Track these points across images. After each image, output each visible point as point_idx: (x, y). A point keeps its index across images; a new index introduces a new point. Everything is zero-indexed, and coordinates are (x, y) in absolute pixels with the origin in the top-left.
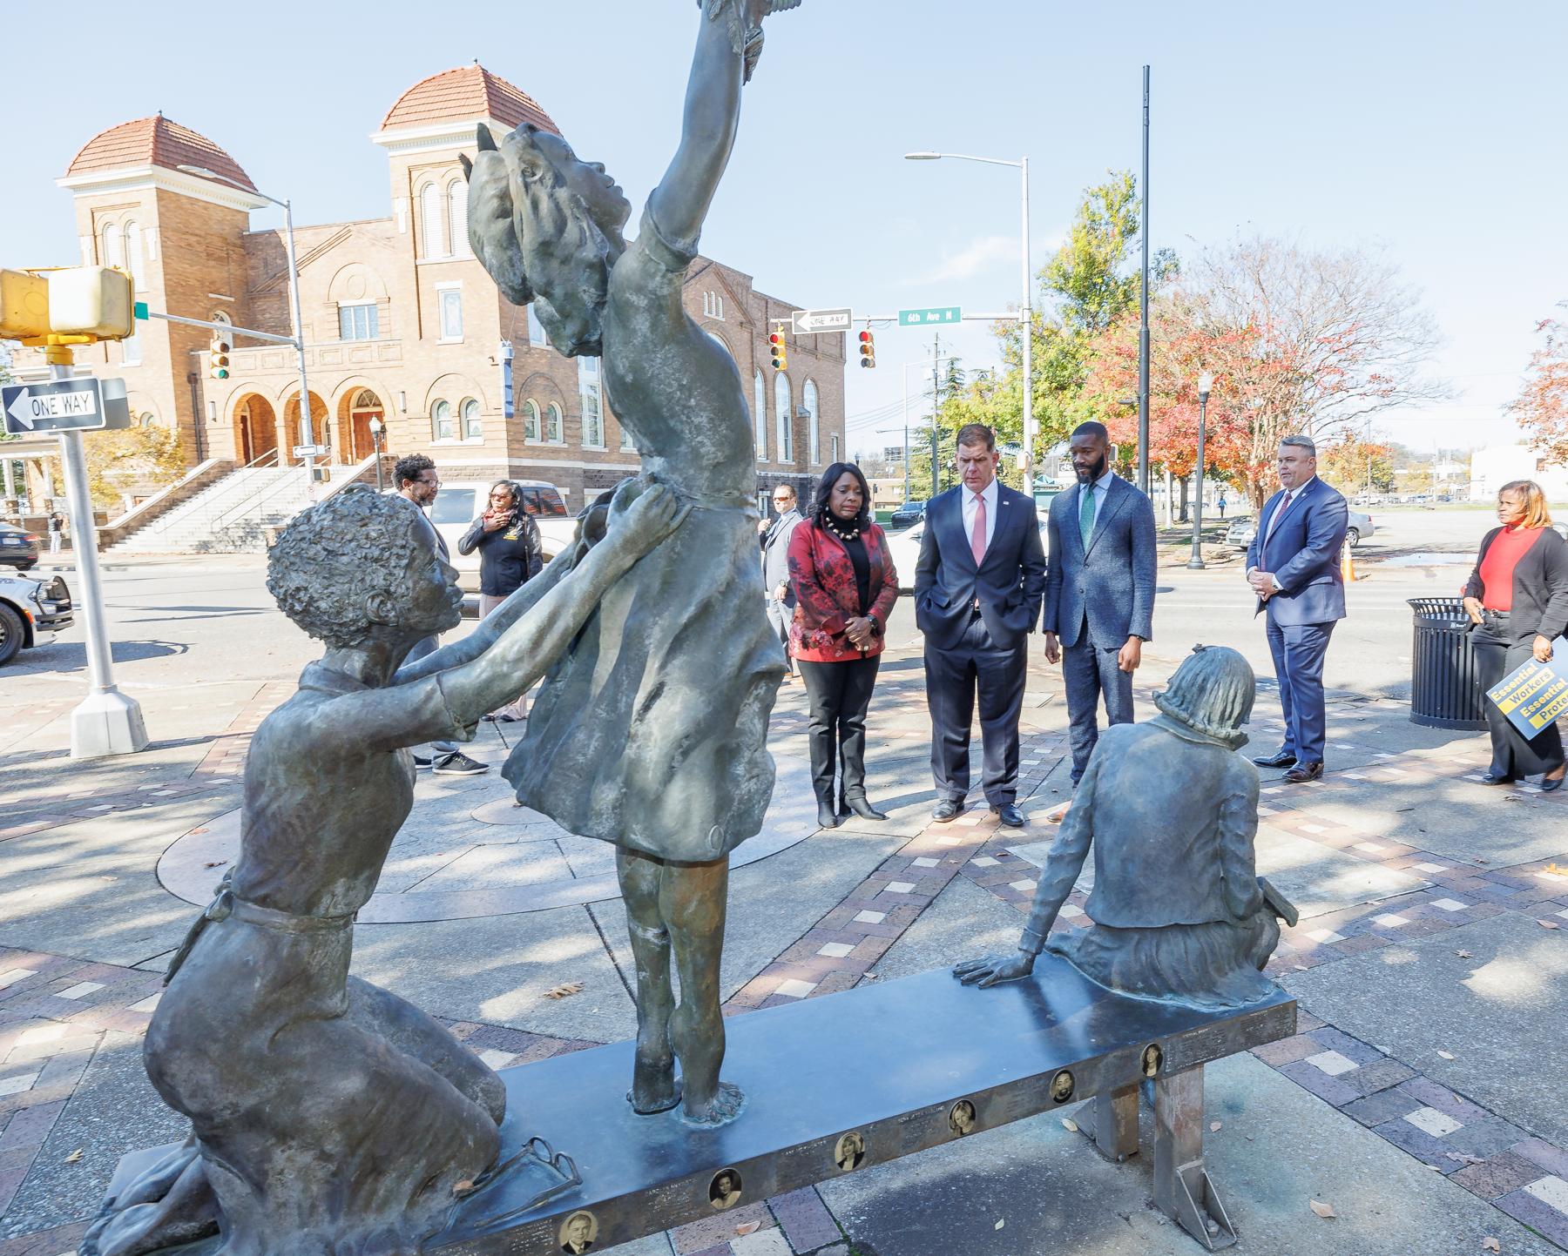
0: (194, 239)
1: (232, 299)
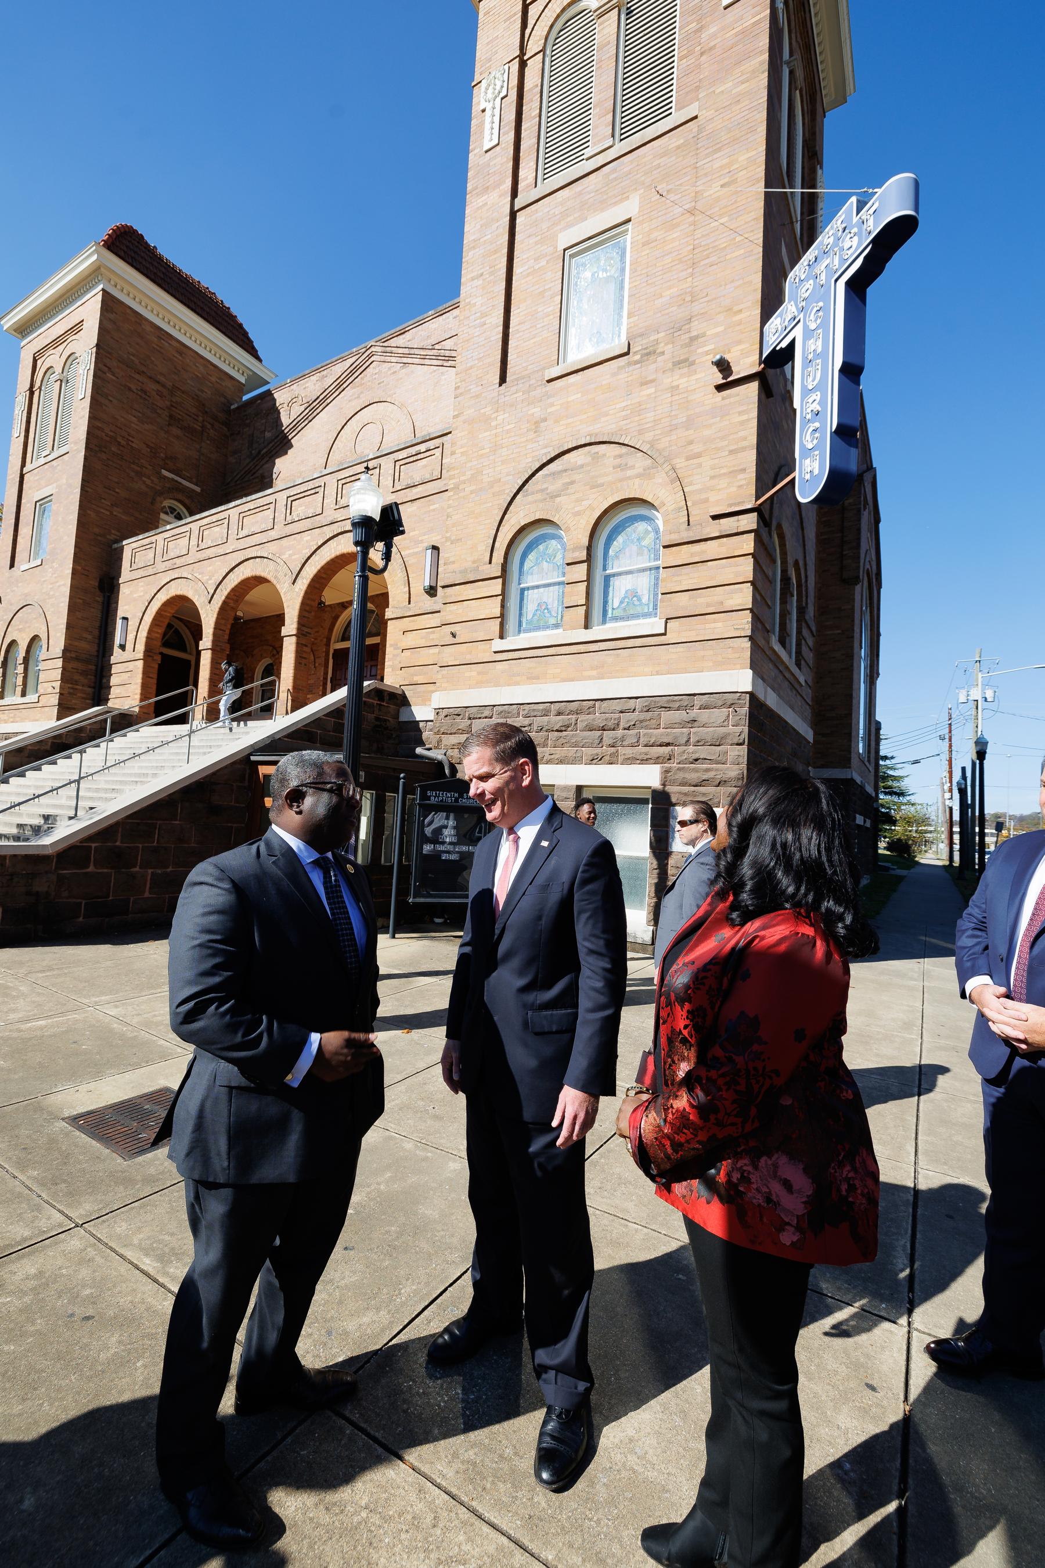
0: (152, 386)
1: (198, 489)
